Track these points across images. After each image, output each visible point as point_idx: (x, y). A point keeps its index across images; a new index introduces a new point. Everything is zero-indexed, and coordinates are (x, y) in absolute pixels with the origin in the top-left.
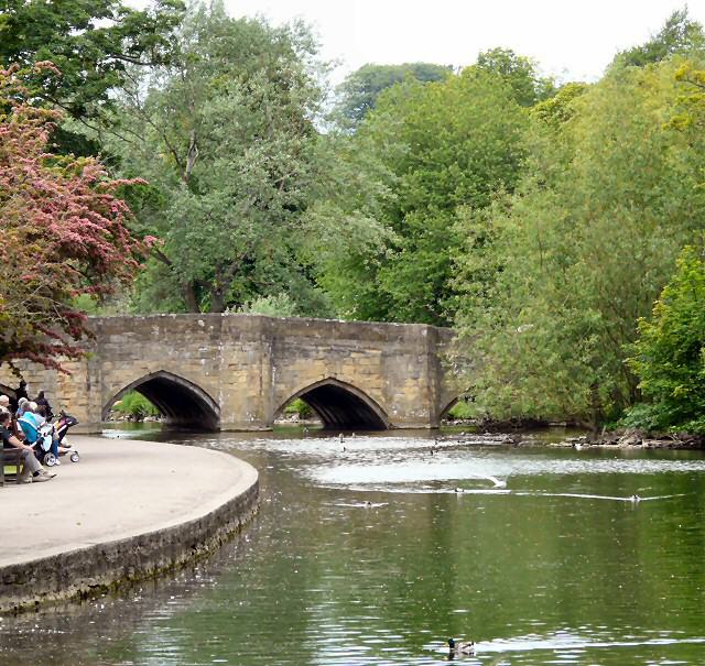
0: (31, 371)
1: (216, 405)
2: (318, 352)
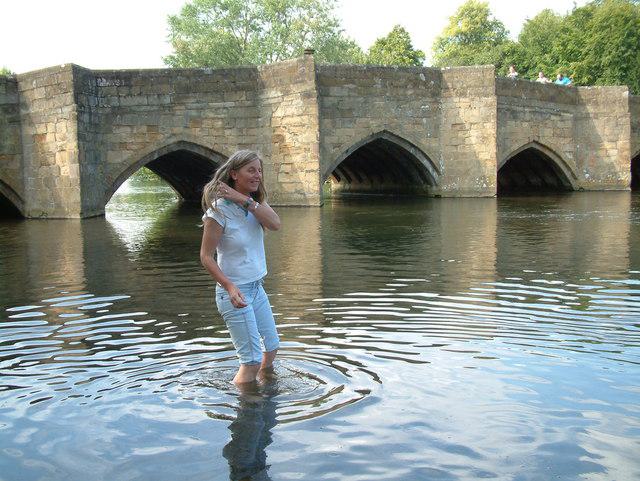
0: (241, 130)
1: (435, 169)
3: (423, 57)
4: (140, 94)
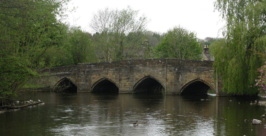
0: (116, 75)
2: (194, 70)
4: (98, 68)
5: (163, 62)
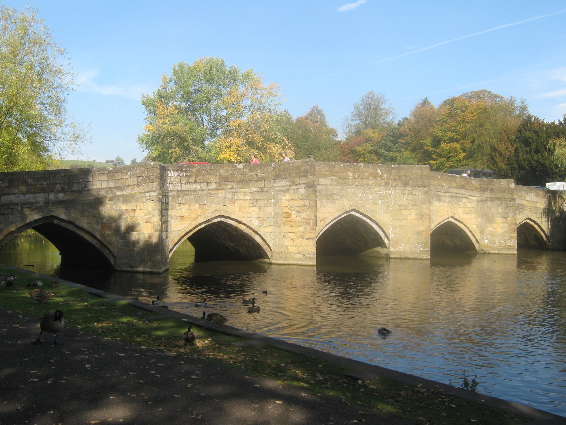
3: (336, 135)
4: (195, 182)
5: (386, 176)
